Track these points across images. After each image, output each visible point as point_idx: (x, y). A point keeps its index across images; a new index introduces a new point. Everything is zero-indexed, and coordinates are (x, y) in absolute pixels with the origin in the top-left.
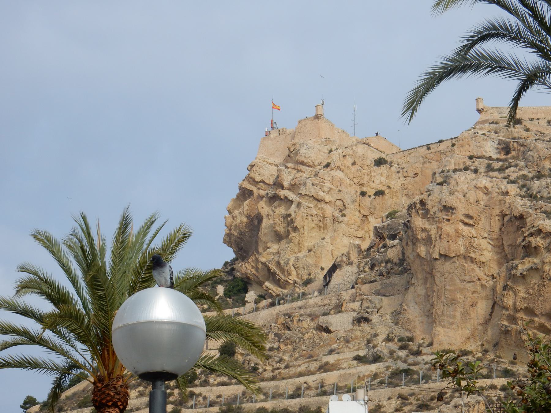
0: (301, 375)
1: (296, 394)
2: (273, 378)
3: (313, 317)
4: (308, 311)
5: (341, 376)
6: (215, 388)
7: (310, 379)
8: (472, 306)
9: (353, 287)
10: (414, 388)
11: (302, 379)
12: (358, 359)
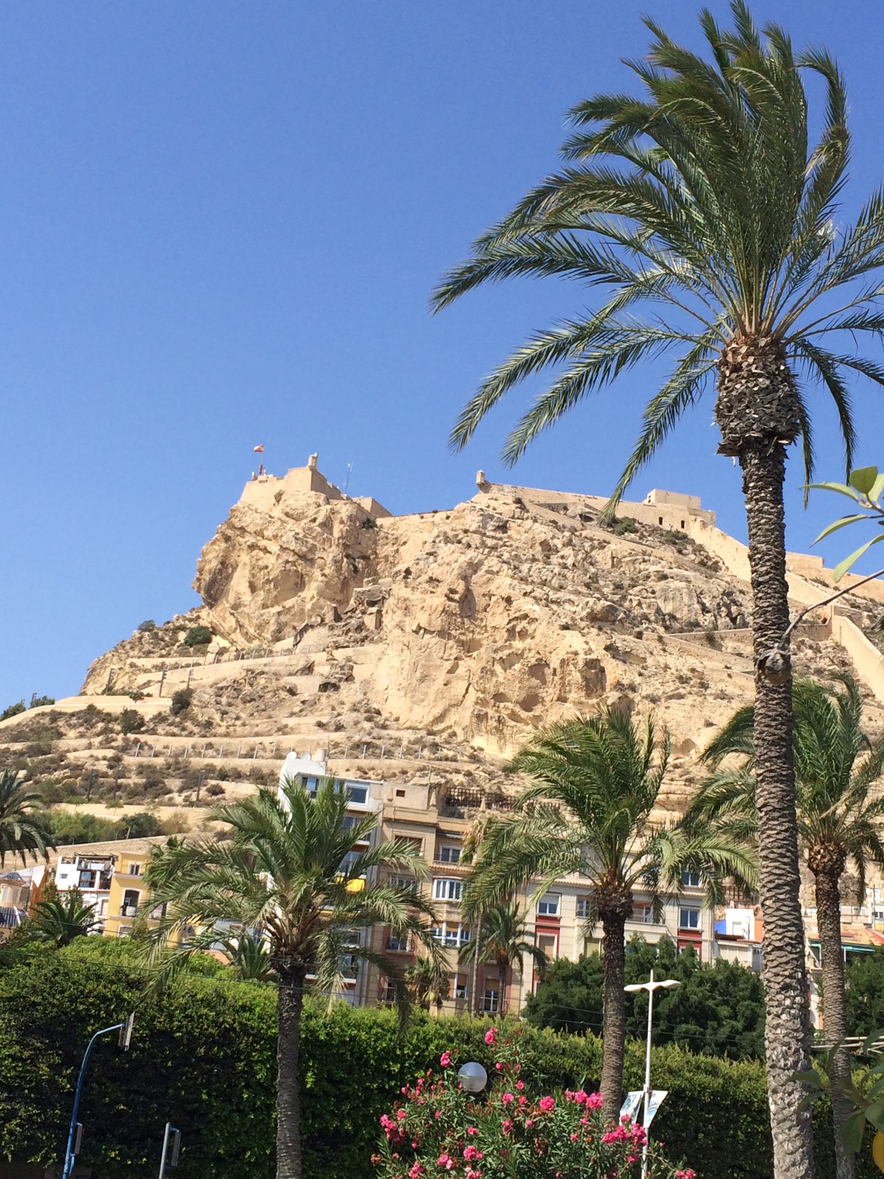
0: (257, 735)
1: (249, 755)
2: (227, 735)
3: (277, 676)
4: (273, 669)
5: (299, 741)
6: (161, 738)
7: (266, 740)
8: (445, 685)
9: (324, 650)
10: (374, 762)
11: (258, 740)
12: (320, 725)
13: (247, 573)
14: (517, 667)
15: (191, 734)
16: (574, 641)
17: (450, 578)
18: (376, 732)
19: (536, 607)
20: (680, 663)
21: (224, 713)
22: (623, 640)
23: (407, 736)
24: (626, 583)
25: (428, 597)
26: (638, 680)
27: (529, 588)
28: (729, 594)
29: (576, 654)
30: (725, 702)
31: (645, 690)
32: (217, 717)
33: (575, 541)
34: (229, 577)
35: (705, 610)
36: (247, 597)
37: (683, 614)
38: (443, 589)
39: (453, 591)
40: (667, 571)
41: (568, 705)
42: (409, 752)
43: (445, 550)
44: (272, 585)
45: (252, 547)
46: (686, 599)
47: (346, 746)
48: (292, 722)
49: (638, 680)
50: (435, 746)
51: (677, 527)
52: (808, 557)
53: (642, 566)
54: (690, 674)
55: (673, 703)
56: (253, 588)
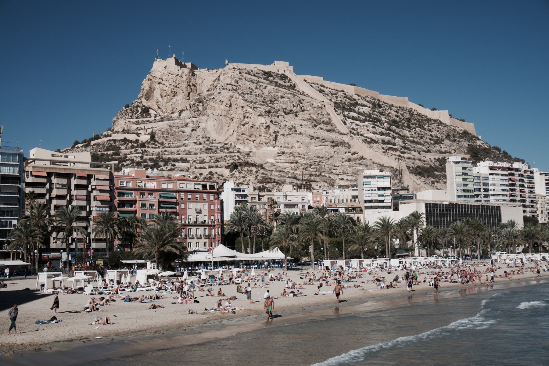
0: (178, 147)
2: (169, 147)
3: (178, 127)
7: (181, 148)
10: (214, 155)
11: (179, 148)
12: (195, 143)
13: (159, 91)
14: (247, 126)
15: (159, 147)
16: (262, 120)
17: (226, 101)
18: (211, 145)
19: (251, 110)
20: (289, 125)
21: (166, 140)
22: (274, 119)
23: (219, 145)
24: (273, 100)
25: (220, 106)
27: (248, 104)
28: (300, 101)
29: (263, 124)
30: (301, 135)
31: (281, 133)
32: (164, 141)
33: (258, 87)
34: (153, 92)
35: (294, 106)
36: (160, 99)
37: (289, 108)
38: (224, 104)
40: (283, 95)
41: (262, 137)
42: (221, 151)
43: (223, 92)
45: (159, 83)
46: (289, 104)
47: (204, 149)
48: (186, 142)
49: (279, 130)
50: (228, 149)
52: (319, 77)
54: (292, 127)
55: (289, 136)
56: (162, 96)
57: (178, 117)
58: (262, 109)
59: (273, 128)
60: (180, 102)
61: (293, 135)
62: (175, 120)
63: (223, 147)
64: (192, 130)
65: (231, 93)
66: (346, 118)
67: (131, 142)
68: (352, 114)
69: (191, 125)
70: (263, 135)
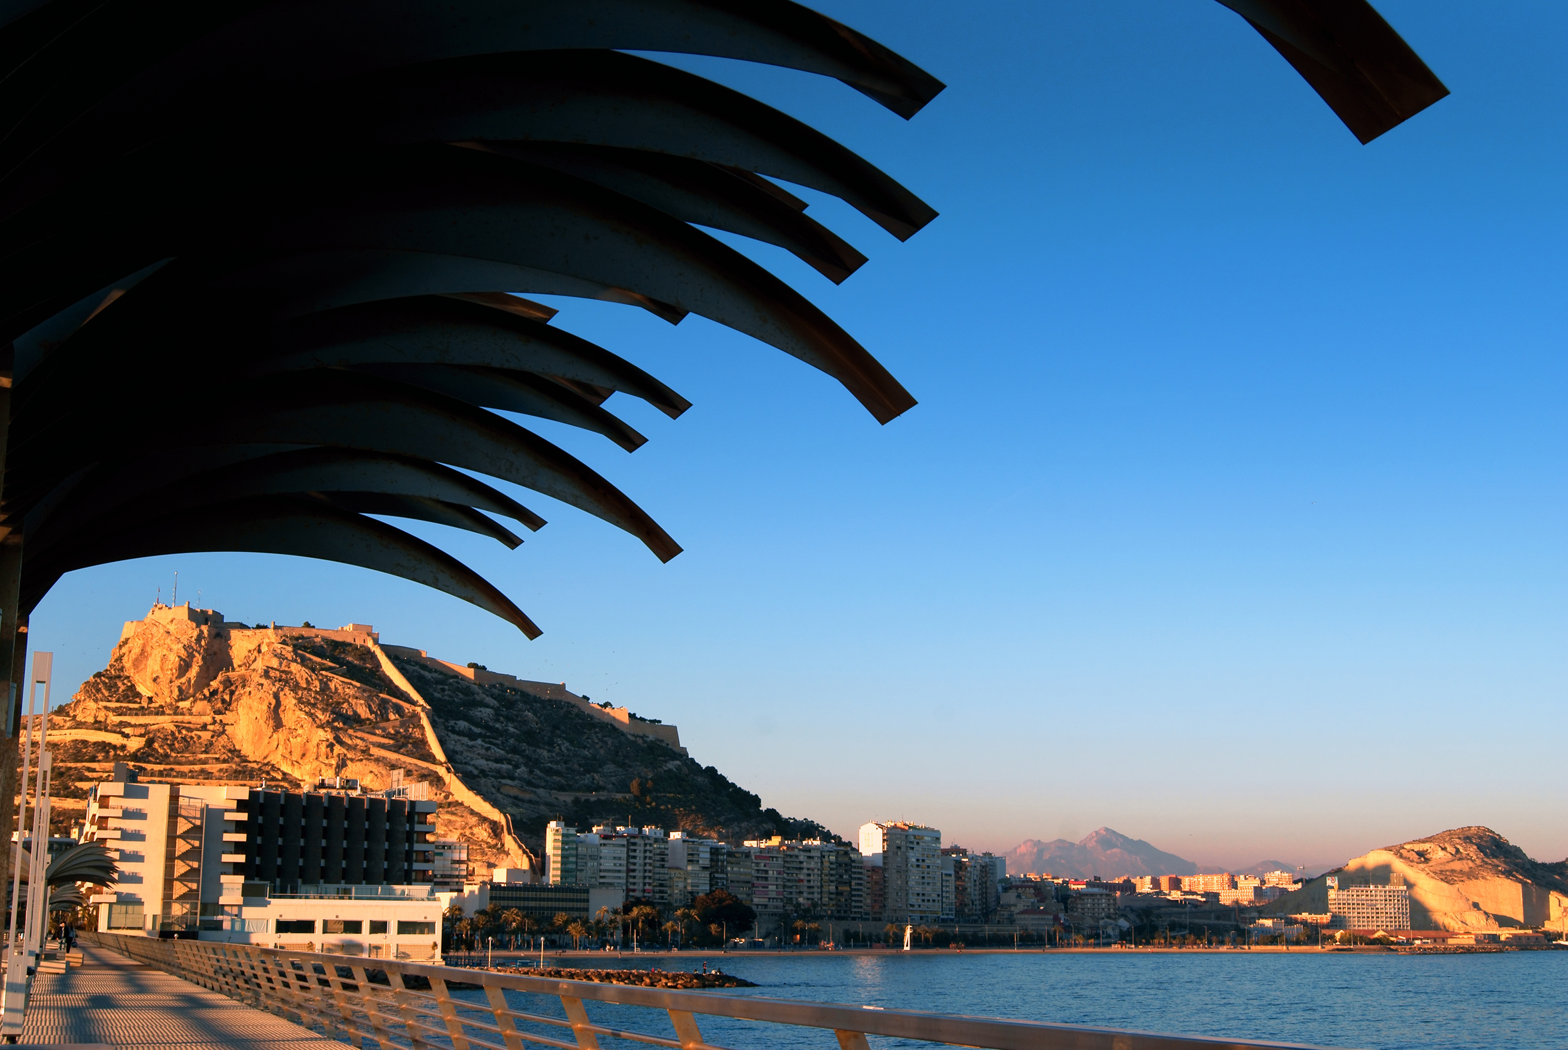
3: (189, 730)
16: (321, 732)
26: (346, 752)
27: (302, 706)
34: (147, 658)
38: (266, 703)
39: (270, 704)
44: (174, 671)
51: (362, 643)
53: (347, 690)
57: (188, 709)
58: (322, 717)
59: (338, 749)
60: (192, 682)
61: (364, 761)
62: (182, 714)
63: (260, 769)
64: (213, 737)
65: (277, 685)
66: (450, 733)
67: (115, 747)
68: (462, 724)
69: (211, 727)
70: (320, 759)
